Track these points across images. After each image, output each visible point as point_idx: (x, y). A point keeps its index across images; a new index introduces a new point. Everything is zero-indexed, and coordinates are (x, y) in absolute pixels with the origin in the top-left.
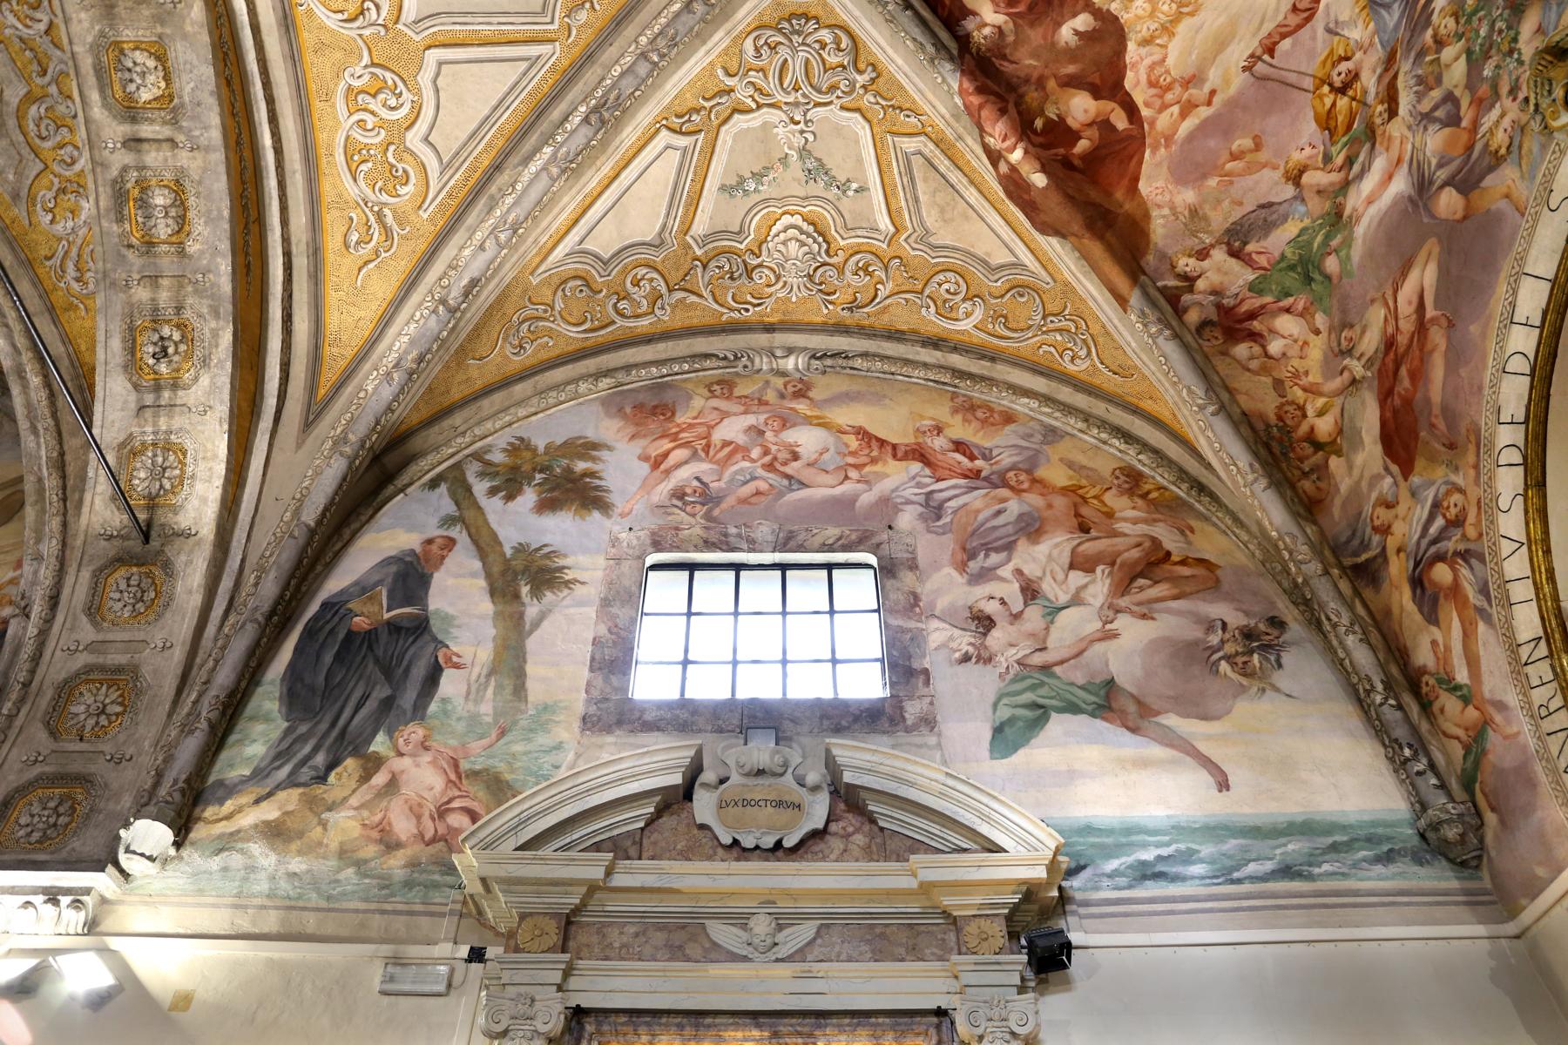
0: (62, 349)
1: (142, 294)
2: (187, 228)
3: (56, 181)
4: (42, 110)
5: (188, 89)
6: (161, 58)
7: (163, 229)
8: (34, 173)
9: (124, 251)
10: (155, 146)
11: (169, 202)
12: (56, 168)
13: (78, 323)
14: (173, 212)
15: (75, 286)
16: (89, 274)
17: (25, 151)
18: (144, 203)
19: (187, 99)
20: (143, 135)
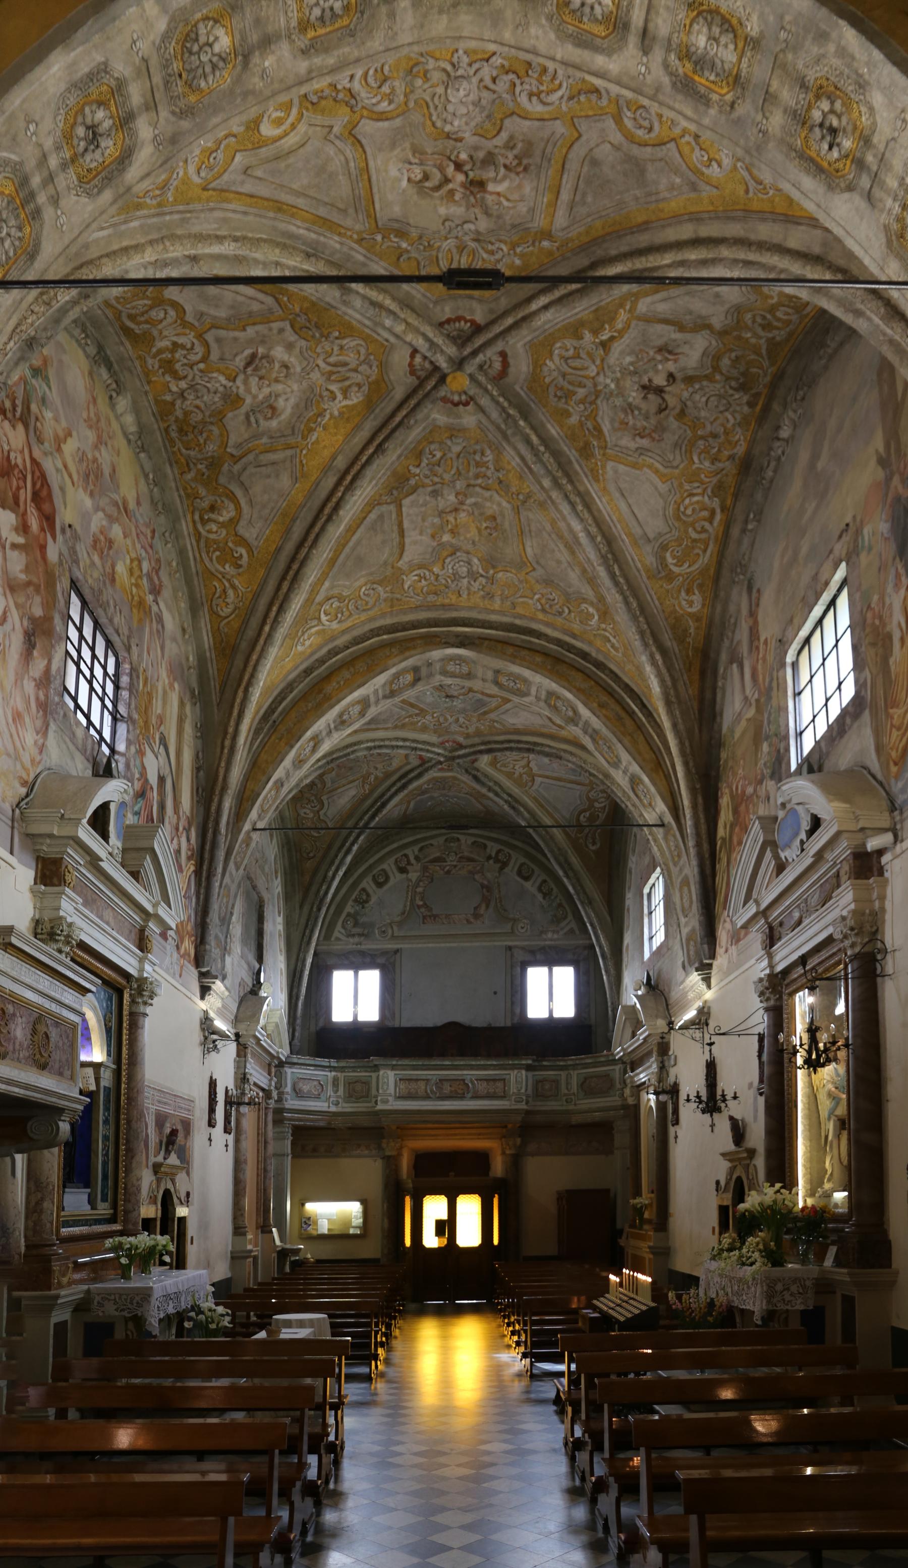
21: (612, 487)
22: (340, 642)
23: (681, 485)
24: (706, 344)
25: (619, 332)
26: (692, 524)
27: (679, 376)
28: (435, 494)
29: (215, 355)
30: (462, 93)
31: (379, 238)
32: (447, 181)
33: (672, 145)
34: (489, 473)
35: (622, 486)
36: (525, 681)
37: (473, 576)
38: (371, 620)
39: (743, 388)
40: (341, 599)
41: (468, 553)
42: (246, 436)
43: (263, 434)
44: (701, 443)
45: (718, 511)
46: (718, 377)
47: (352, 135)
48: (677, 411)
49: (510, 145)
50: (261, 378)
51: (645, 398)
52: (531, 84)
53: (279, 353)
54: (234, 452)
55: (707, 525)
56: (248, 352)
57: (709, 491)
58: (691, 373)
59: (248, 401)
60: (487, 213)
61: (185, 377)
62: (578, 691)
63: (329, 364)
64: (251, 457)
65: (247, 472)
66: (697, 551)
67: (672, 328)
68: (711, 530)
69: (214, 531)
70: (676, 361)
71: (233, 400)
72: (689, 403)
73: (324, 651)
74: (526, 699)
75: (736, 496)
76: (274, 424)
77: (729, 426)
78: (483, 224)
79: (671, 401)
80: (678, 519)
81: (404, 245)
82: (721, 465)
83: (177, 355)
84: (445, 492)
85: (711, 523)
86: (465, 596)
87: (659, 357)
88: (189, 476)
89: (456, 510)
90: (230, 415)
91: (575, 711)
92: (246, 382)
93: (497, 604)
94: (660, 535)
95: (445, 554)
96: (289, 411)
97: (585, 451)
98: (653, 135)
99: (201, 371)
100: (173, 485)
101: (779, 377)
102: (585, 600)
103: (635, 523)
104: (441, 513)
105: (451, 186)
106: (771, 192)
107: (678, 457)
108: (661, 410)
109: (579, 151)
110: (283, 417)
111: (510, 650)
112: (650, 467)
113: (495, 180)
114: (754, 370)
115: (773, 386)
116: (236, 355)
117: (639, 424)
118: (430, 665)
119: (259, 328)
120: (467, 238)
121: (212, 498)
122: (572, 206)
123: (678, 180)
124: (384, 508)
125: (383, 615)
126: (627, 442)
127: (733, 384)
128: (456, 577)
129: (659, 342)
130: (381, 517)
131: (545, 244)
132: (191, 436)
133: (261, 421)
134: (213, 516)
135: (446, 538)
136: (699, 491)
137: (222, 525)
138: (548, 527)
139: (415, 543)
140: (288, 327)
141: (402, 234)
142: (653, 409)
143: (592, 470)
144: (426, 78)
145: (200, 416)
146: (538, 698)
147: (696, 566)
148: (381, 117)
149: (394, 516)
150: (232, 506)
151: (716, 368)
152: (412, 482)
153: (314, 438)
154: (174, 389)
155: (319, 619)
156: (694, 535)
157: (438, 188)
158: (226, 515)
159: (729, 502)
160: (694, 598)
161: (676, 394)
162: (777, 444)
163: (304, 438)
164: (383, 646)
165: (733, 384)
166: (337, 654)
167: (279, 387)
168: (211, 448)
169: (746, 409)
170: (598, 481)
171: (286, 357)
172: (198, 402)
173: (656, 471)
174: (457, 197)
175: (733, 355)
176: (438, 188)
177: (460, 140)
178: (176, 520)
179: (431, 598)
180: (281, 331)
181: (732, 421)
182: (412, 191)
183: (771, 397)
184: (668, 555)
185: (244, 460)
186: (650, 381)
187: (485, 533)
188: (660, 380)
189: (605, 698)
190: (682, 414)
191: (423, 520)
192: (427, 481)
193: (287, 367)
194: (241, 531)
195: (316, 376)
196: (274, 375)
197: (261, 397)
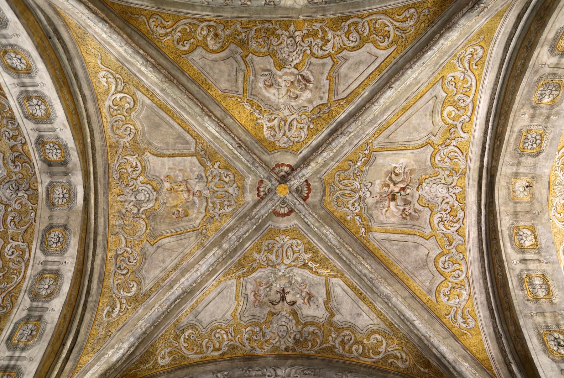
0: (465, 352)
1: (539, 319)
2: (551, 292)
3: (450, 284)
4: (447, 258)
5: (543, 241)
6: (533, 231)
7: (541, 293)
8: (440, 282)
9: (526, 302)
10: (532, 262)
11: (541, 283)
12: (451, 279)
13: (469, 341)
14: (544, 287)
15: (463, 325)
16: (469, 320)
17: (437, 274)
18: (531, 283)
19: (543, 245)
20: (527, 258)
21: (222, 285)
22: (90, 104)
23: (231, 325)
24: (320, 316)
25: (316, 272)
26: (210, 340)
27: (295, 307)
28: (200, 177)
29: (313, 60)
30: (441, 190)
31: (366, 152)
32: (395, 184)
33: (443, 279)
34: (216, 210)
35: (224, 292)
36: (62, 251)
37: (138, 204)
38: (102, 131)
39: (297, 342)
40: (129, 110)
41: (156, 200)
42: (256, 67)
43: (255, 77)
44: (258, 329)
45: (220, 352)
46: (300, 327)
47: (429, 144)
48: (274, 311)
49: (415, 210)
50: (292, 83)
51: (277, 292)
52: (446, 218)
53: (307, 95)
54: (248, 58)
55: (211, 349)
56: (312, 79)
57: (231, 343)
58: (299, 313)
59: (279, 73)
60: (377, 203)
61: (303, 41)
62: (69, 295)
63: (293, 120)
64: (243, 67)
65: (235, 63)
66: (195, 348)
67: (325, 297)
68: (208, 352)
69: (202, 32)
70: (304, 303)
71: (281, 64)
72: (280, 316)
73: (87, 92)
74: (39, 253)
75: (231, 359)
76: (261, 85)
77: (271, 341)
78: (370, 201)
79: (279, 307)
80: (212, 331)
81: (359, 164)
82: (247, 344)
83: (319, 40)
84: (201, 184)
85: (213, 351)
86: (119, 199)
87: (304, 294)
88: (238, 26)
89: (189, 191)
90: (272, 61)
91: (50, 297)
92: (292, 74)
93: (115, 222)
94: (201, 322)
95: (154, 185)
96: (267, 94)
97: (239, 266)
98: (443, 270)
99: (305, 51)
100: (235, 15)
101: (309, 357)
102: (139, 284)
103: (204, 305)
104: (186, 181)
105: (392, 185)
106: (456, 325)
107: (247, 319)
108: (272, 302)
109: (420, 240)
110: (264, 91)
111: (84, 236)
112: (238, 305)
113: (396, 205)
114: (310, 344)
115: (302, 356)
116: (311, 72)
117: (262, 292)
118: (66, 174)
119: (327, 87)
120: (361, 193)
121: (223, 37)
122: (389, 240)
123: (427, 284)
124: (193, 146)
125: (104, 140)
126: (250, 288)
127: (298, 336)
128: (136, 192)
129: (314, 293)
130: (187, 143)
131: (363, 230)
132: (263, 35)
133: (264, 78)
134: (212, 34)
135: (167, 185)
136: (230, 337)
137: (205, 39)
138: (187, 251)
139: (163, 164)
140: (323, 102)
141: (365, 163)
142: (271, 298)
143: (229, 271)
144: (448, 176)
145: (274, 43)
146: (45, 263)
147: (186, 351)
148: (433, 157)
149: (186, 151)
150: (215, 48)
151: (305, 325)
152: (209, 164)
153: (247, 107)
154: (297, 33)
155: (121, 92)
156: (204, 344)
157: (391, 180)
158: (210, 42)
159: (226, 356)
160: (167, 358)
161: (284, 308)
162: (272, 371)
163: (248, 101)
164: (84, 138)
165: (298, 336)
166: (83, 101)
167: (283, 91)
168: (254, 45)
169: (283, 347)
170: (224, 276)
171: (303, 98)
172: (285, 44)
173: (236, 309)
174: (386, 189)
175: (317, 331)
176: (391, 180)
177: (418, 189)
178: (213, 9)
179: (116, 175)
180: (321, 98)
181: (274, 342)
182: (390, 168)
183: (294, 357)
184: (190, 331)
185: (242, 63)
186: (288, 292)
187: (174, 210)
188: (289, 298)
189: (68, 318)
190: (272, 314)
191: (180, 170)
192: (209, 172)
193: (296, 98)
194: (199, 50)
195: (286, 113)
196: (292, 90)
197: (280, 80)
